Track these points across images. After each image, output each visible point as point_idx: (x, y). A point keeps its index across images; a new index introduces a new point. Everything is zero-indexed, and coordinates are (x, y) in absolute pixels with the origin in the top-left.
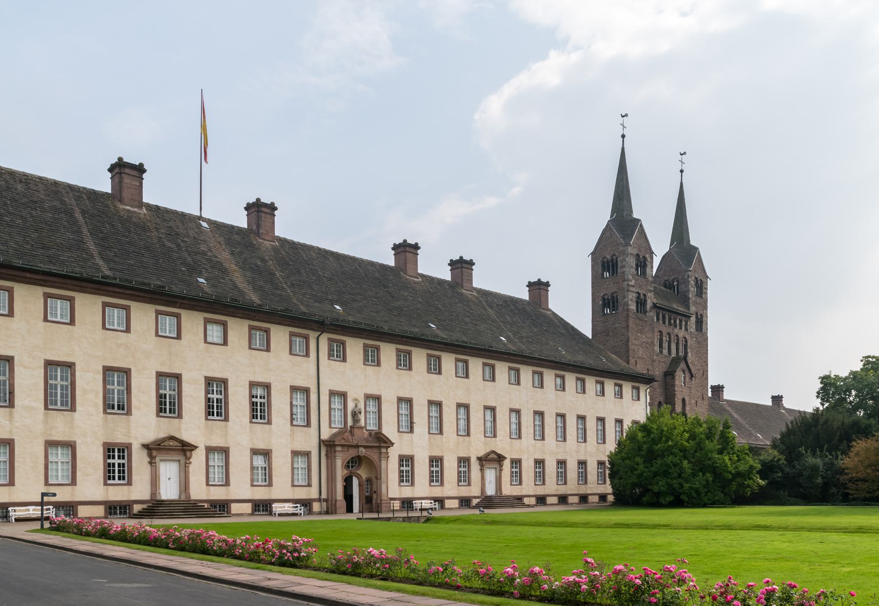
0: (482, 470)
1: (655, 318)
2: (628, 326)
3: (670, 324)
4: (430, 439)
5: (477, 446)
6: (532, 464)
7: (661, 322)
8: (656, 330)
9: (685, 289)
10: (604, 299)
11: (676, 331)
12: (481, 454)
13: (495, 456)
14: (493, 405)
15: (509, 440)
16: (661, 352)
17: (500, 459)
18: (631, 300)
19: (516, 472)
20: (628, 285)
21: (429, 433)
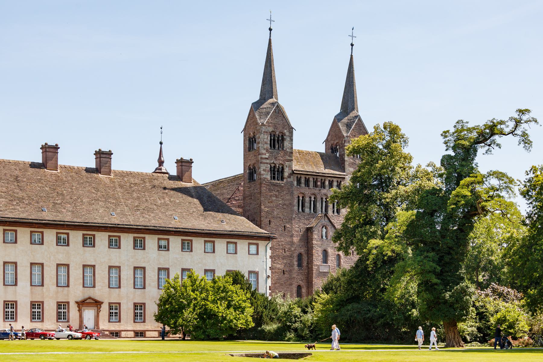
0: (80, 310)
1: (295, 183)
2: (260, 193)
3: (315, 185)
4: (31, 289)
5: (76, 292)
6: (132, 307)
7: (303, 185)
8: (296, 193)
9: (342, 153)
10: (250, 169)
11: (324, 191)
12: (80, 299)
13: (93, 301)
14: (93, 264)
15: (108, 289)
16: (303, 211)
17: (97, 304)
18: (264, 170)
19: (116, 313)
20: (261, 158)
21: (31, 285)
